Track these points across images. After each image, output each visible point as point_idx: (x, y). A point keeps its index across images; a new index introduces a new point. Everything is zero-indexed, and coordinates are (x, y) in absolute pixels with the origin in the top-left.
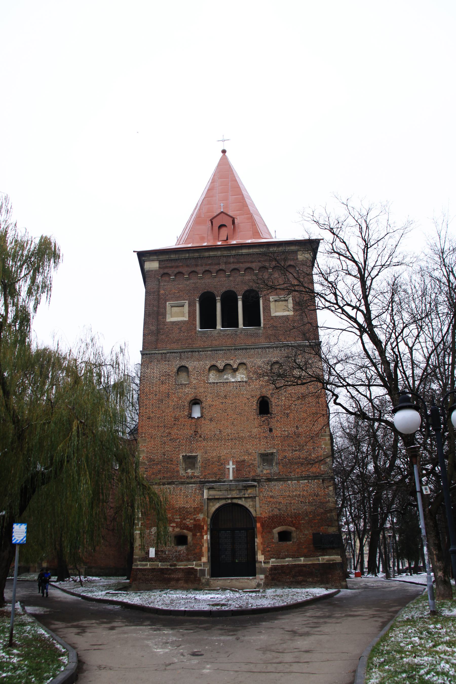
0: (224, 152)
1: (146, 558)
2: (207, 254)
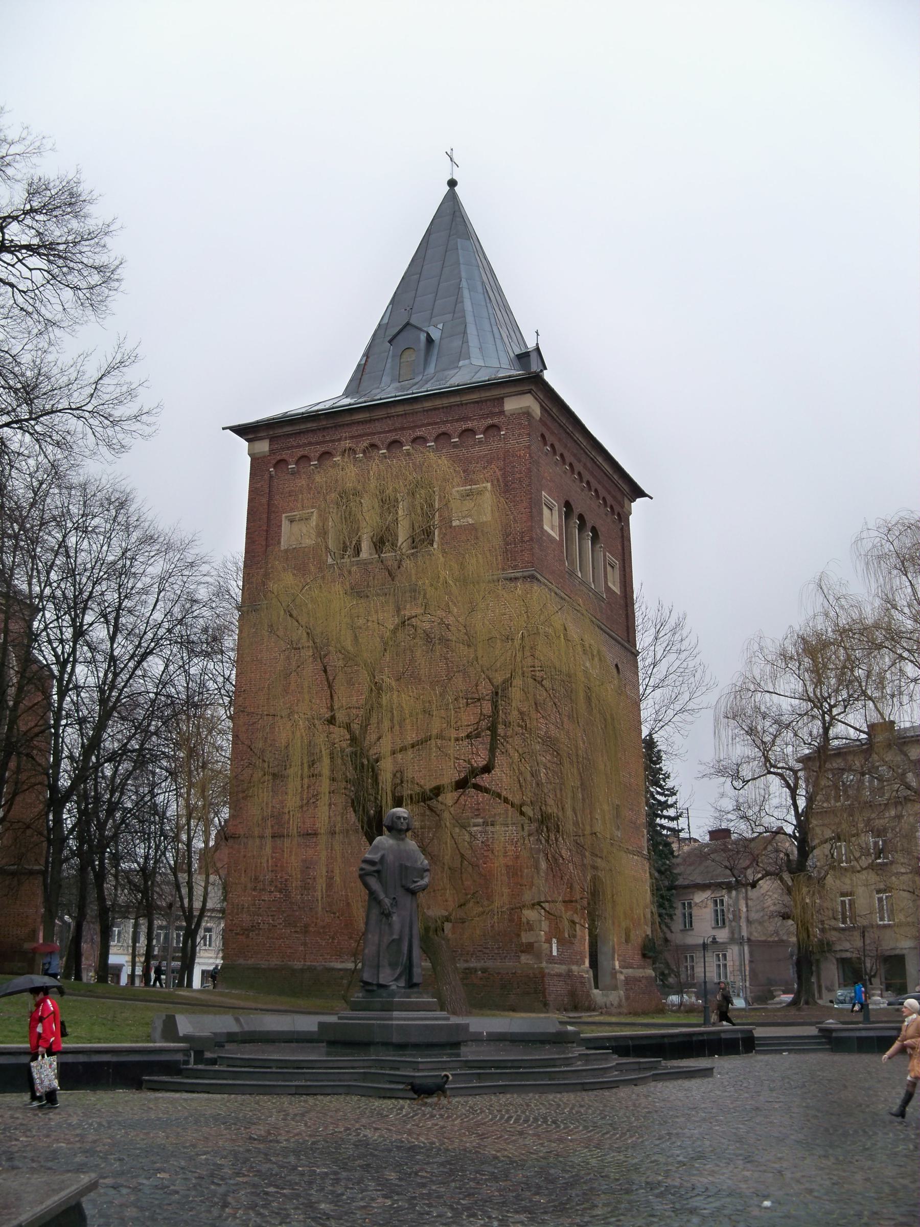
0: (452, 183)
1: (551, 959)
2: (578, 436)
